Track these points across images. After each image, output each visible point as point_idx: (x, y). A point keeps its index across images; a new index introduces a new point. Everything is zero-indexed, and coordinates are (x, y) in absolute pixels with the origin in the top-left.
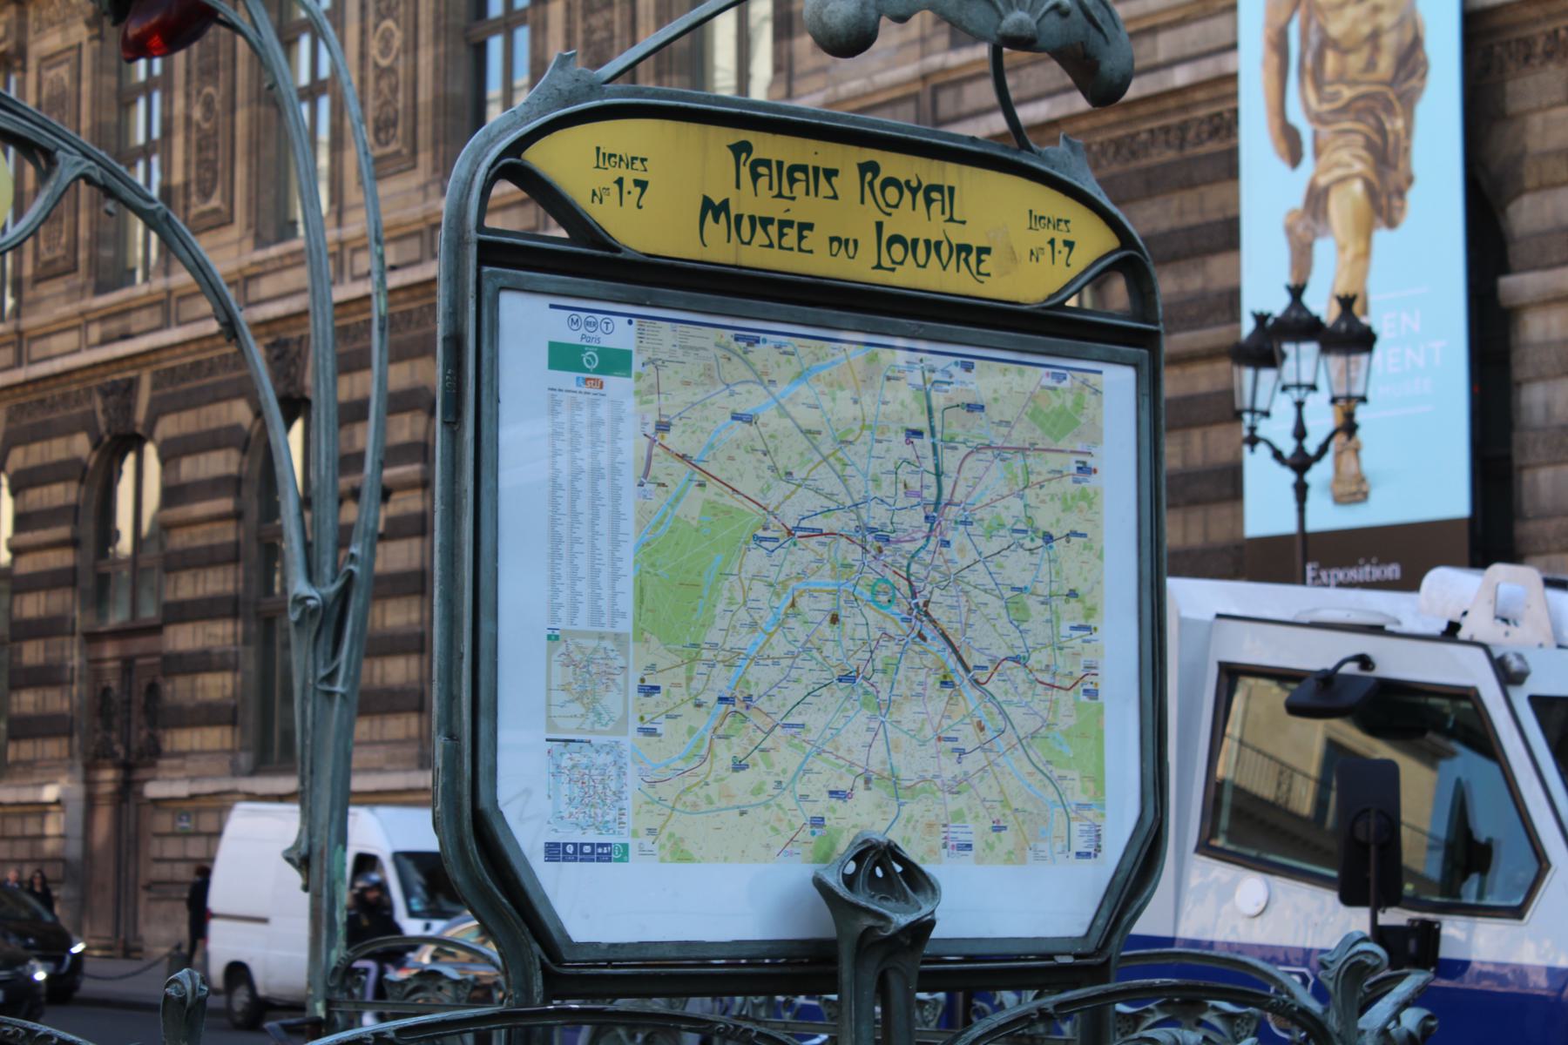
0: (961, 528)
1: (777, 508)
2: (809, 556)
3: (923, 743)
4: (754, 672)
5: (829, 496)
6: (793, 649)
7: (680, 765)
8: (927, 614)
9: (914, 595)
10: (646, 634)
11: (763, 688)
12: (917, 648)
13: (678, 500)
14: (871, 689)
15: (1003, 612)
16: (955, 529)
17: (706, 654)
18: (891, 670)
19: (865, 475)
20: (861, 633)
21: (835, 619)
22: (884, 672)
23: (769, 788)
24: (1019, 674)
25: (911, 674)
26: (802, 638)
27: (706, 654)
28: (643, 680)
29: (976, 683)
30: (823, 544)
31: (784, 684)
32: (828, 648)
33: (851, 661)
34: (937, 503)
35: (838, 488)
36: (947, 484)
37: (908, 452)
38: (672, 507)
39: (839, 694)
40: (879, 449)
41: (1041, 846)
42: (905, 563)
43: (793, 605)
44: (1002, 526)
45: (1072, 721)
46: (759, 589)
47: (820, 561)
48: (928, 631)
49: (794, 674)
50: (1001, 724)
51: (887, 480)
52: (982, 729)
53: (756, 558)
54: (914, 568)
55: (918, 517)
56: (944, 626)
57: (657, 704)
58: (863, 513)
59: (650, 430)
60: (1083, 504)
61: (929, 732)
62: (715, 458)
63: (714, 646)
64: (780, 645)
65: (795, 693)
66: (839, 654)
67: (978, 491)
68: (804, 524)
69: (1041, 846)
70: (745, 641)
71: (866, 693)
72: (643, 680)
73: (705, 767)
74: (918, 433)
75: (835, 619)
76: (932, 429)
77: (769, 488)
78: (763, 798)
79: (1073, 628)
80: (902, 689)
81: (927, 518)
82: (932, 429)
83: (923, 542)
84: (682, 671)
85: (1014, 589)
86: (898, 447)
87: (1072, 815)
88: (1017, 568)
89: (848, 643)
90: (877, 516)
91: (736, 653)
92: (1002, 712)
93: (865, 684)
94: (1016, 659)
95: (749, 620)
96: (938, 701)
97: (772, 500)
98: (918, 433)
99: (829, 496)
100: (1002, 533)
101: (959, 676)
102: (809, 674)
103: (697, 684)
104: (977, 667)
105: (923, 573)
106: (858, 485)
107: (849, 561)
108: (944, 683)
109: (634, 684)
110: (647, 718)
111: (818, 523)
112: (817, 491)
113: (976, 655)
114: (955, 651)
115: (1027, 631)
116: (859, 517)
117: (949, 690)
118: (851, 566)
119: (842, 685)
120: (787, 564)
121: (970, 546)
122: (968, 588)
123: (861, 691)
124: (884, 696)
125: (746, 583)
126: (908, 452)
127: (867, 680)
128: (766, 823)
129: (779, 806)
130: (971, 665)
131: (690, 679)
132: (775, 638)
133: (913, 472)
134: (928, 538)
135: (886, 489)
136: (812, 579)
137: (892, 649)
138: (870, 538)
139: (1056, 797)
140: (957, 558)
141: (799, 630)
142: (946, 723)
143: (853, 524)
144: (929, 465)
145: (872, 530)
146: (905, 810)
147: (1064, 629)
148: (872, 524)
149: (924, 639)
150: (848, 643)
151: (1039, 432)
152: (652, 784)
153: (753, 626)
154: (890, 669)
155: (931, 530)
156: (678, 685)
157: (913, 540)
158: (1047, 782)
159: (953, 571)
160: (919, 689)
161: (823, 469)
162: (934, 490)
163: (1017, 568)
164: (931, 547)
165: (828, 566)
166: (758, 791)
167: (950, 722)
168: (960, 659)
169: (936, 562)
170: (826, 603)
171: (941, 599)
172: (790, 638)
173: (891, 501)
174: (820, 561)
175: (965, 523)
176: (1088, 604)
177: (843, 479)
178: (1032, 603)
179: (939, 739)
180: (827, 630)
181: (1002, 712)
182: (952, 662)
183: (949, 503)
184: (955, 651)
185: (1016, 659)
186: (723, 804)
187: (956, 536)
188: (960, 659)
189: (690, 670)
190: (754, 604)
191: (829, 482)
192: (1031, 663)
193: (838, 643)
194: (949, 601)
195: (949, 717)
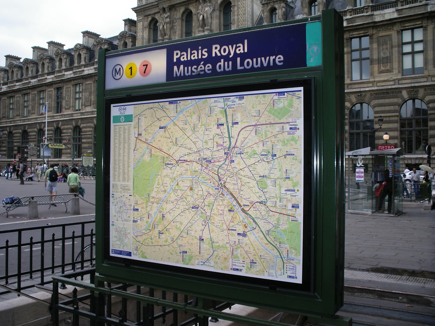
0: (239, 155)
1: (173, 155)
2: (183, 169)
3: (223, 231)
4: (165, 206)
5: (190, 149)
6: (177, 198)
7: (144, 231)
8: (225, 187)
9: (220, 180)
10: (135, 194)
11: (167, 210)
12: (221, 198)
13: (144, 155)
14: (203, 212)
15: (256, 185)
16: (236, 157)
17: (151, 200)
18: (211, 206)
19: (202, 141)
20: (201, 193)
21: (191, 189)
22: (209, 206)
23: (169, 240)
24: (263, 208)
25: (219, 207)
26: (180, 195)
27: (151, 200)
28: (134, 207)
29: (243, 210)
30: (188, 165)
31: (174, 209)
32: (189, 198)
33: (197, 202)
34: (229, 148)
35: (193, 146)
36: (233, 141)
37: (218, 131)
38: (142, 157)
39: (192, 213)
40: (207, 133)
41: (271, 271)
42: (217, 169)
43: (177, 184)
44: (256, 154)
45: (286, 226)
46: (167, 180)
47: (187, 170)
48: (225, 192)
49: (177, 206)
50: (254, 225)
51: (210, 142)
52: (246, 227)
53: (167, 171)
54: (220, 170)
55: (222, 153)
56: (231, 191)
57: (138, 214)
58: (202, 154)
59: (136, 136)
60: (293, 142)
61: (225, 227)
62: (154, 141)
63: (154, 197)
64: (173, 197)
65: (178, 212)
66: (193, 200)
67: (245, 142)
68: (181, 159)
69: (271, 271)
70: (162, 195)
71: (202, 213)
72: (134, 207)
73: (151, 233)
74: (222, 125)
75: (191, 189)
76: (227, 122)
77: (170, 148)
78: (167, 243)
79: (285, 191)
80: (215, 211)
81: (225, 153)
82: (227, 122)
83: (224, 161)
84: (144, 205)
85: (260, 177)
86: (215, 130)
87: (285, 261)
88: (262, 168)
89: (195, 196)
90: (207, 154)
91: (160, 199)
92: (254, 221)
93: (202, 210)
94: (261, 203)
95: (163, 190)
96: (228, 216)
97: (171, 152)
98: (223, 125)
99: (190, 149)
100: (256, 156)
101: (237, 208)
102: (182, 206)
103: (148, 209)
104: (244, 205)
105: (223, 172)
106: (200, 145)
107: (197, 169)
108: (230, 211)
109: (132, 208)
110: (135, 217)
111: (186, 158)
112: (185, 148)
113: (244, 200)
114: (236, 199)
115: (266, 192)
116: (200, 155)
117: (232, 213)
118: (197, 171)
119: (193, 210)
120: (176, 172)
121: (242, 162)
122: (240, 177)
123: (200, 212)
124: (208, 214)
125: (163, 178)
126: (218, 131)
127: (202, 209)
128: (169, 251)
129: (173, 247)
130: (242, 204)
131: (147, 207)
132: (171, 195)
133: (220, 138)
134: (226, 160)
135: (210, 145)
136: (184, 176)
137: (212, 199)
138: (204, 161)
139: (278, 254)
140: (237, 166)
141: (180, 193)
142: (232, 224)
143: (198, 158)
144: (226, 135)
145: (204, 159)
146: (215, 253)
147: (283, 191)
148: (205, 157)
149: (223, 195)
150: (195, 196)
151: (272, 117)
152: (137, 236)
153: (165, 191)
154: (211, 205)
155: (227, 157)
156: (144, 208)
157: (219, 161)
158: (274, 248)
159: (235, 171)
160: (221, 212)
161: (188, 141)
162: (228, 143)
163: (262, 168)
164: (227, 163)
165: (189, 172)
166: (166, 241)
167: (232, 224)
168: (238, 202)
169: (229, 168)
170: (188, 184)
171: (230, 181)
172: (176, 195)
173: (212, 149)
174: (187, 170)
175: (240, 153)
176: (295, 181)
177: (195, 143)
178: (269, 182)
179: (229, 230)
180: (189, 192)
181: (254, 221)
182: (235, 203)
183: (234, 147)
184: (236, 199)
185: (261, 203)
186: (156, 244)
187: (237, 159)
188: (238, 202)
189: (147, 204)
190: (165, 185)
191: (189, 144)
192: (268, 204)
193: (192, 196)
194: (233, 182)
195: (233, 222)
